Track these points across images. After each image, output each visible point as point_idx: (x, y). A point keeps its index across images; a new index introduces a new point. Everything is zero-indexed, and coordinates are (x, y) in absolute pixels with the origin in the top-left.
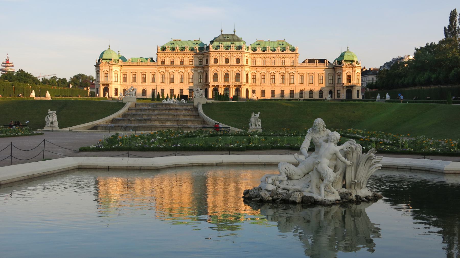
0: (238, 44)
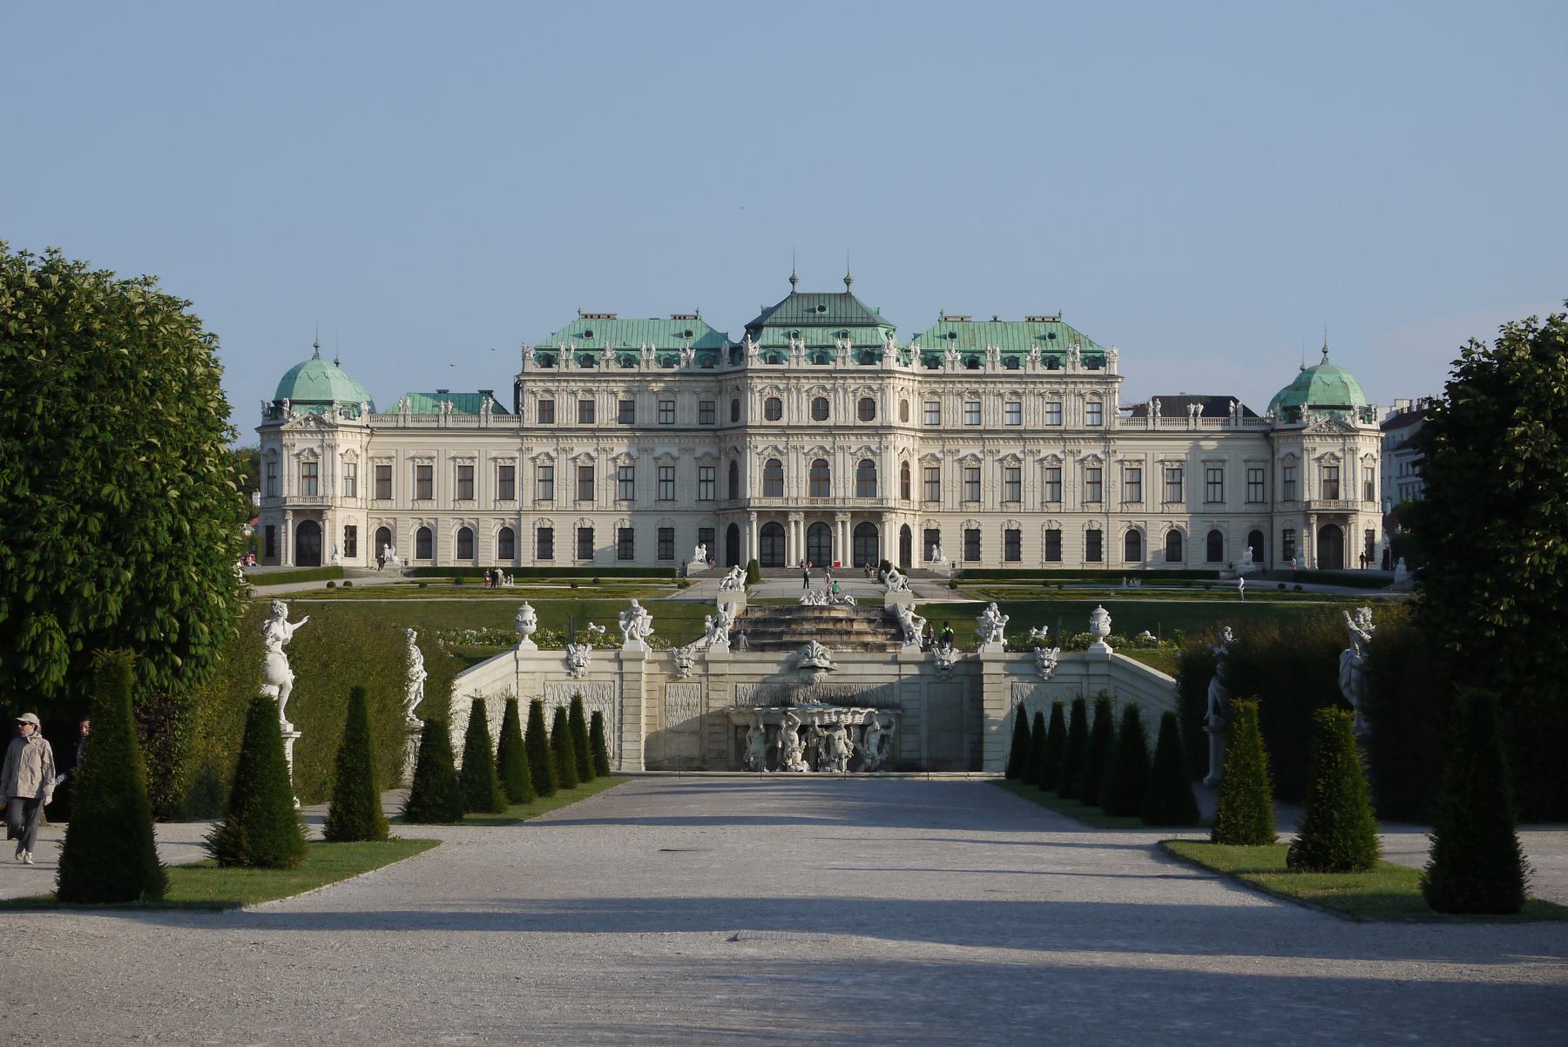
0: (863, 336)
